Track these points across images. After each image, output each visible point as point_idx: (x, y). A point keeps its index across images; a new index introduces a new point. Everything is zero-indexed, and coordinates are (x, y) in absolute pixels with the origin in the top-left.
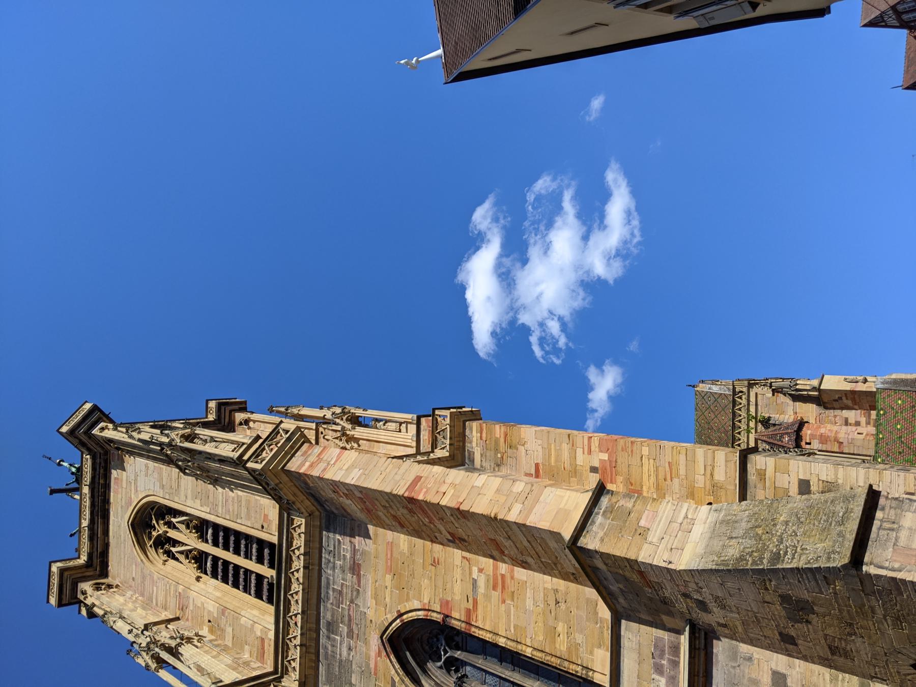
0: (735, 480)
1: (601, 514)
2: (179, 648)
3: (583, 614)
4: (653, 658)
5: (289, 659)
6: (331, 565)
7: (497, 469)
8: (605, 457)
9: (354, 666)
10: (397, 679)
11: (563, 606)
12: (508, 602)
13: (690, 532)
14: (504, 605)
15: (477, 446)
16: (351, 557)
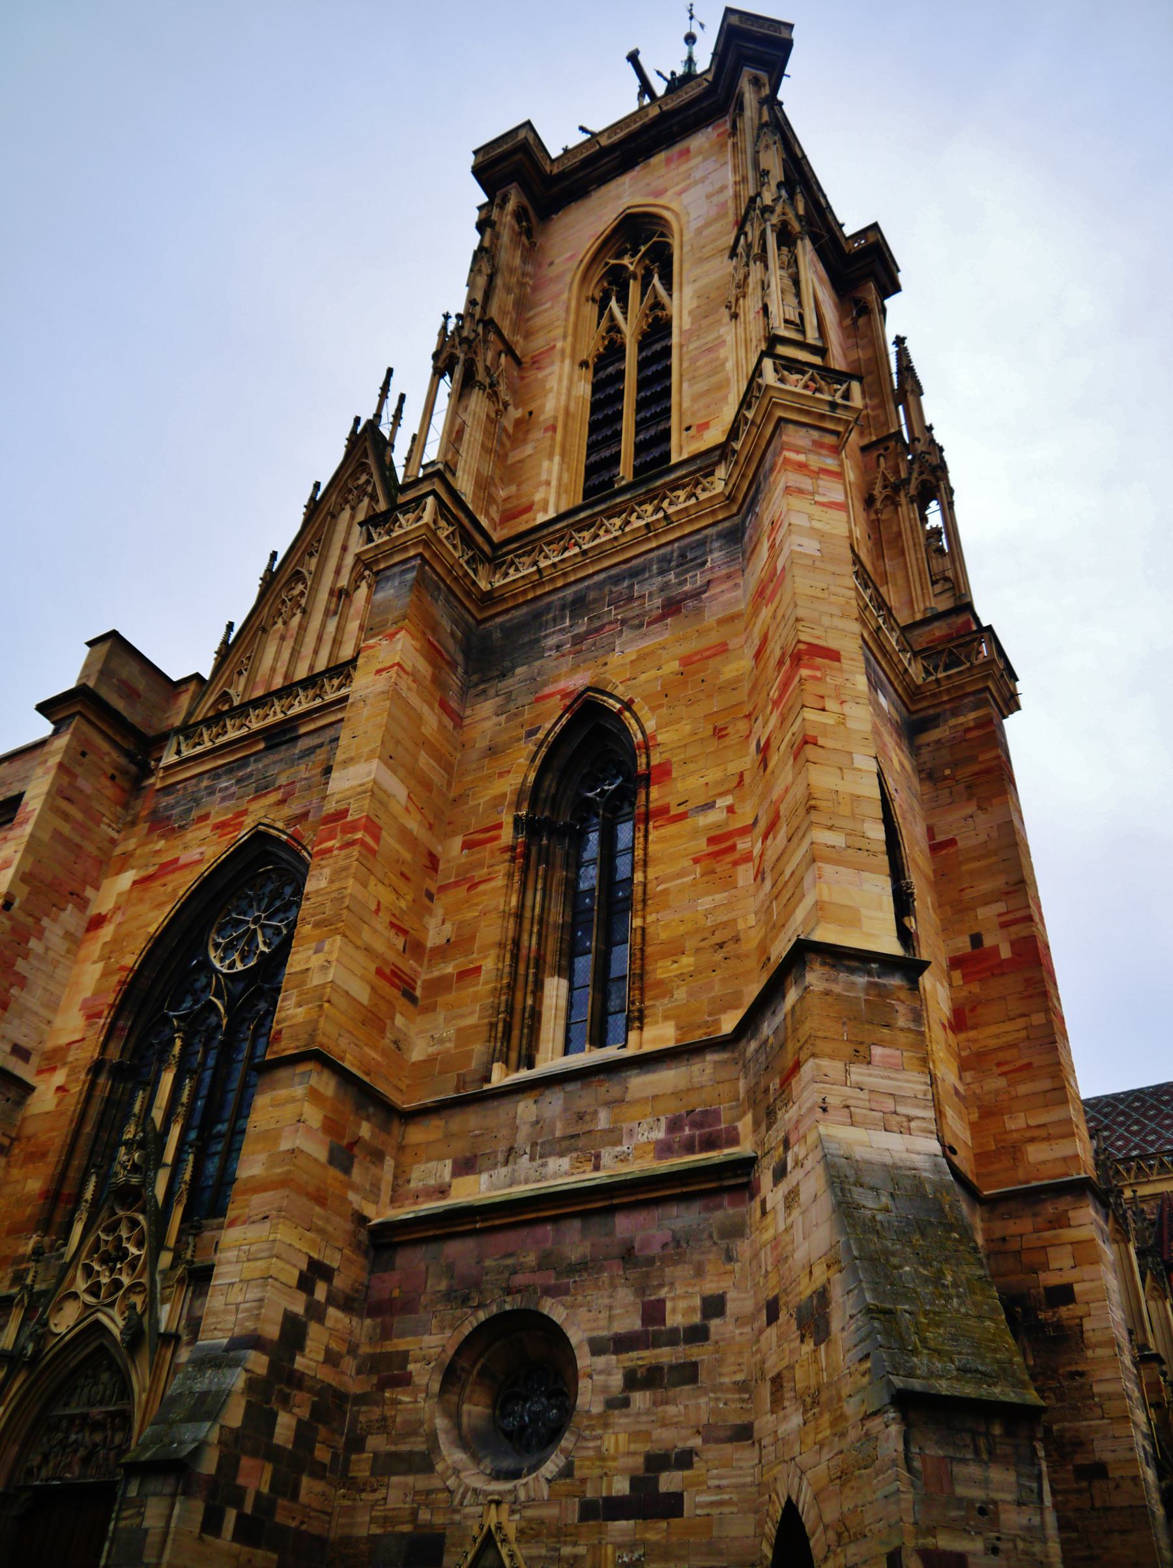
0: (1037, 1179)
1: (871, 979)
3: (718, 990)
4: (688, 1113)
5: (517, 561)
6: (665, 566)
7: (923, 775)
8: (1005, 953)
9: (537, 663)
10: (540, 735)
11: (719, 956)
12: (698, 869)
13: (886, 1130)
14: (691, 862)
15: (950, 728)
16: (686, 593)
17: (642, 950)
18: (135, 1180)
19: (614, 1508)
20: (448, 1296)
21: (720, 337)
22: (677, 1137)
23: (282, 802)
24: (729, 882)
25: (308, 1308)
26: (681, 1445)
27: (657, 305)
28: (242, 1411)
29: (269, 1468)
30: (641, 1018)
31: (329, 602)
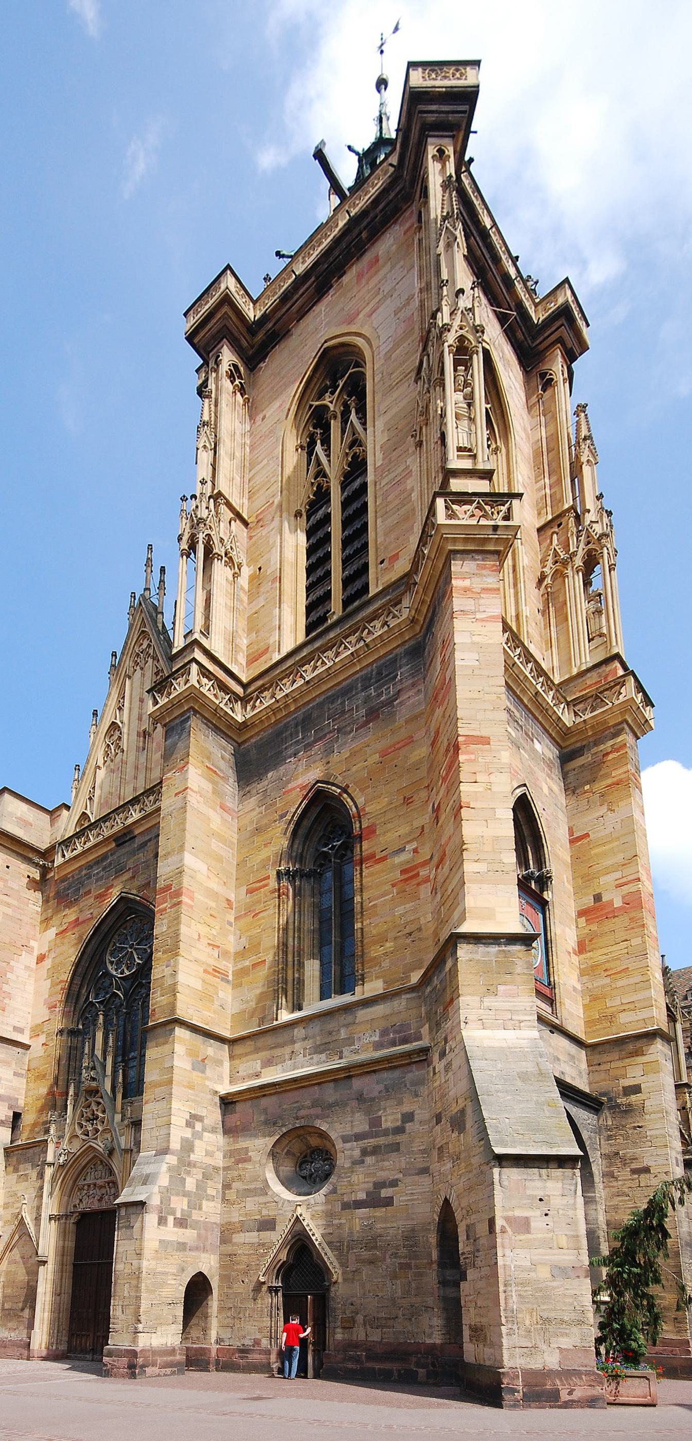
2: (216, 560)
17: (362, 942)
18: (94, 1084)
19: (358, 1204)
20: (266, 1122)
21: (407, 467)
22: (386, 1039)
23: (133, 877)
24: (415, 897)
25: (193, 1135)
26: (391, 1178)
27: (356, 442)
28: (168, 1179)
29: (185, 1200)
30: (363, 979)
31: (138, 741)
